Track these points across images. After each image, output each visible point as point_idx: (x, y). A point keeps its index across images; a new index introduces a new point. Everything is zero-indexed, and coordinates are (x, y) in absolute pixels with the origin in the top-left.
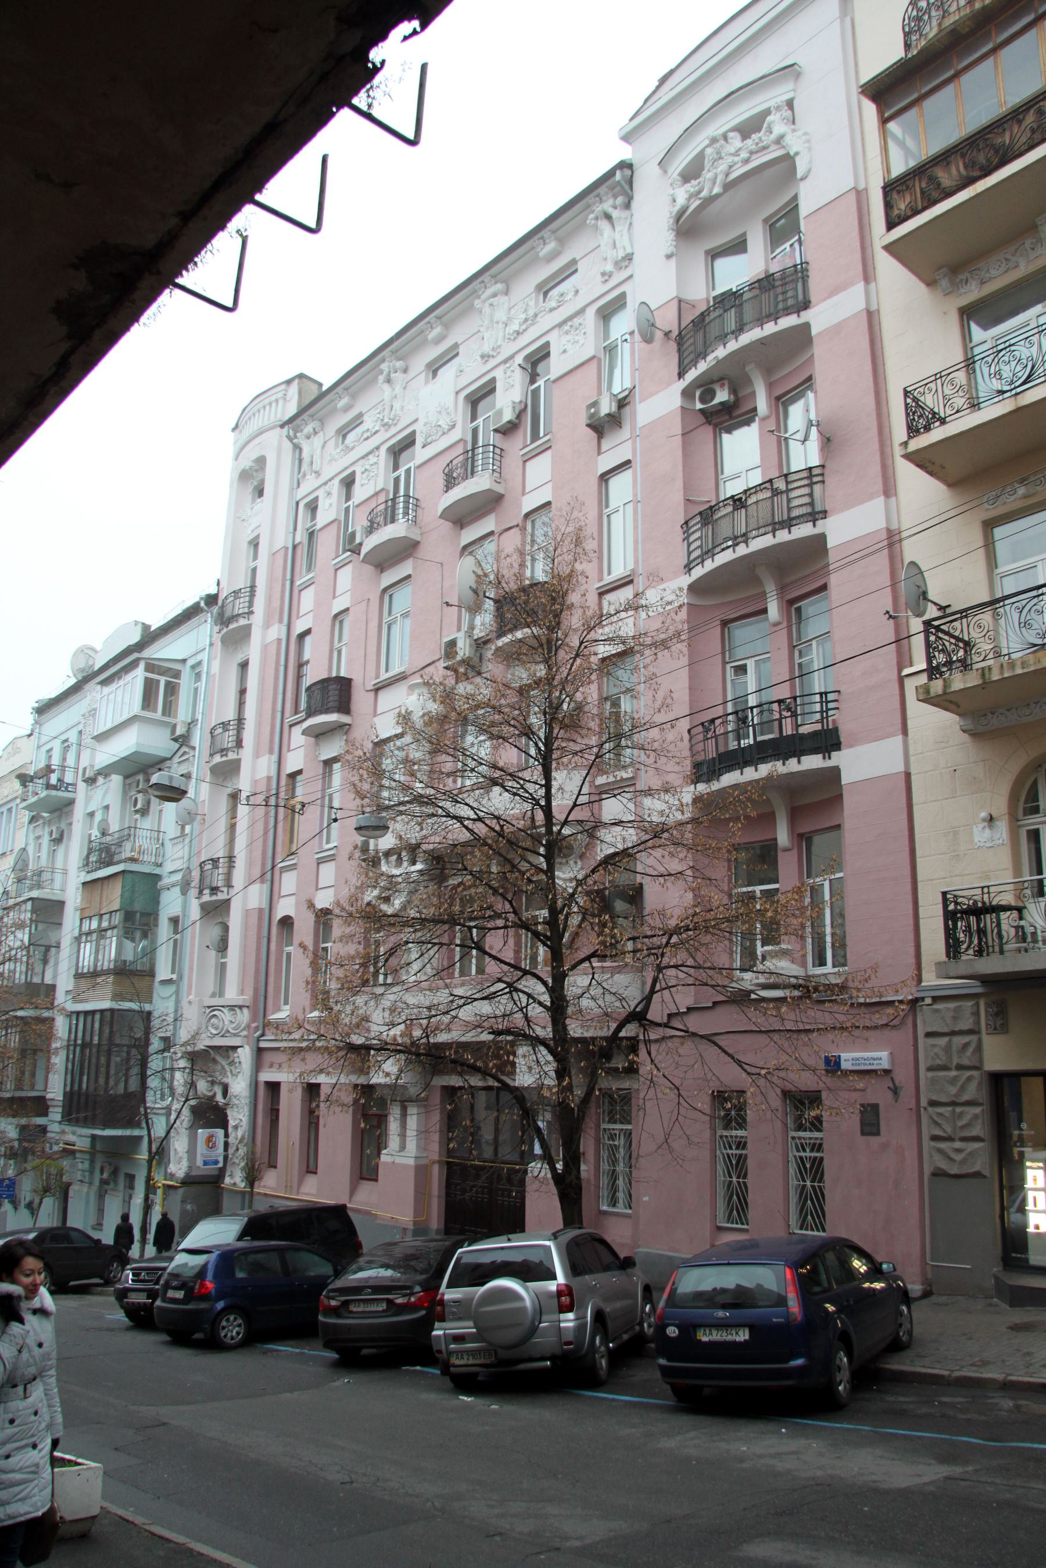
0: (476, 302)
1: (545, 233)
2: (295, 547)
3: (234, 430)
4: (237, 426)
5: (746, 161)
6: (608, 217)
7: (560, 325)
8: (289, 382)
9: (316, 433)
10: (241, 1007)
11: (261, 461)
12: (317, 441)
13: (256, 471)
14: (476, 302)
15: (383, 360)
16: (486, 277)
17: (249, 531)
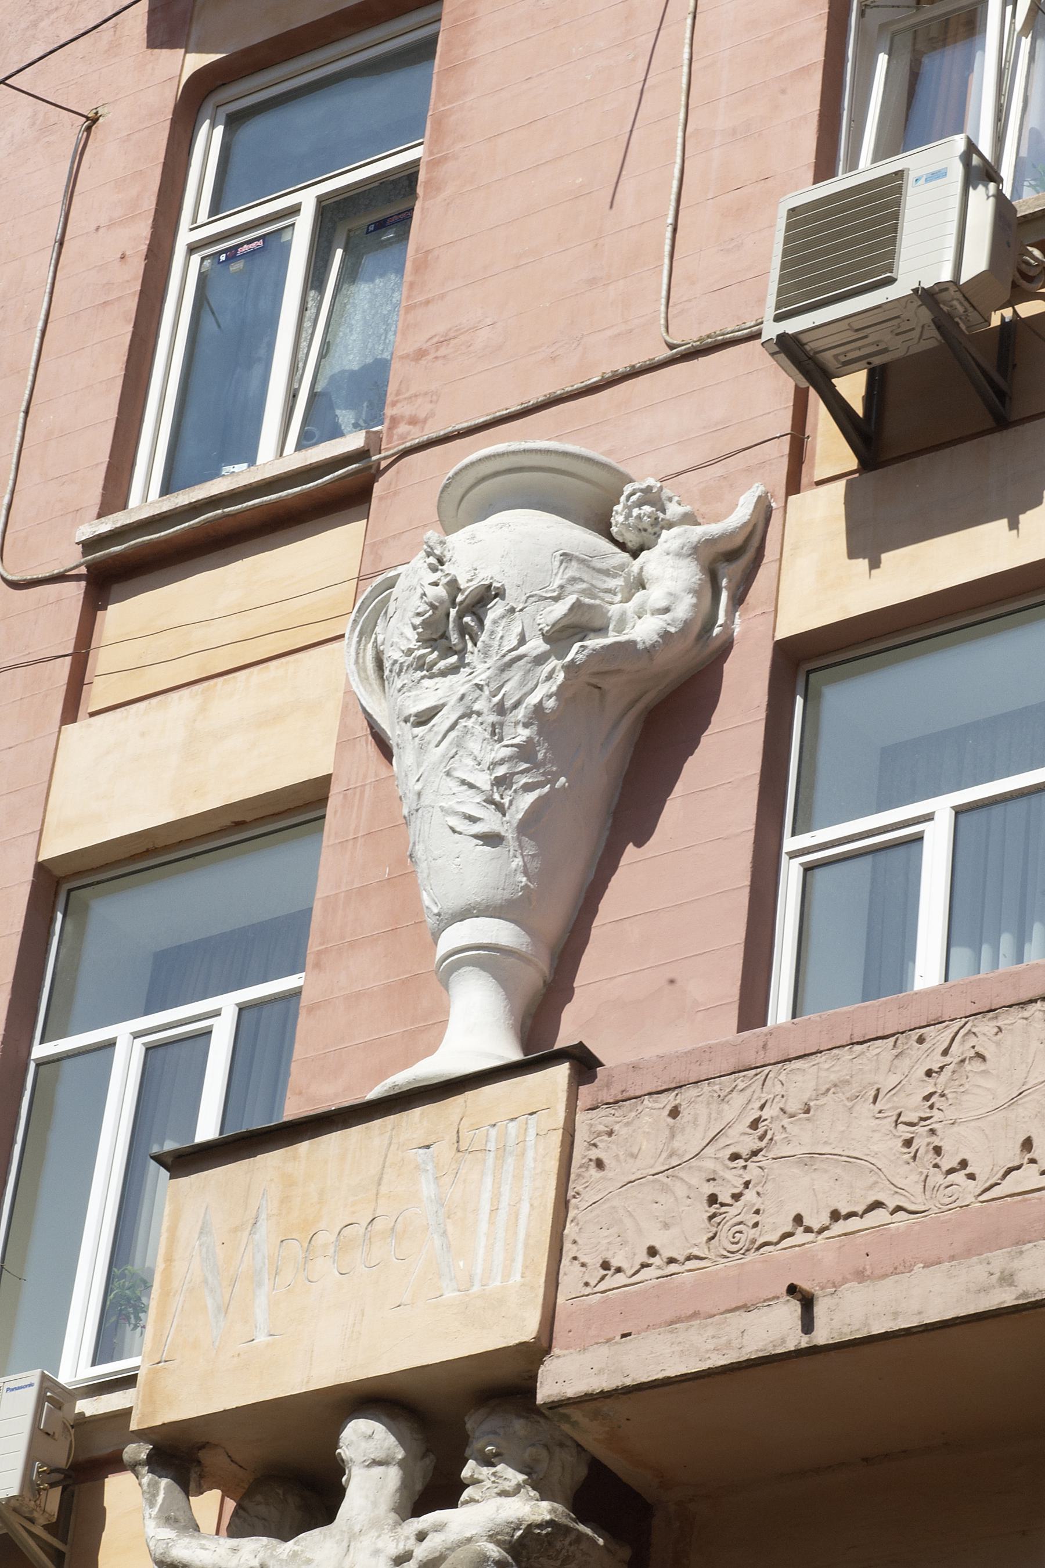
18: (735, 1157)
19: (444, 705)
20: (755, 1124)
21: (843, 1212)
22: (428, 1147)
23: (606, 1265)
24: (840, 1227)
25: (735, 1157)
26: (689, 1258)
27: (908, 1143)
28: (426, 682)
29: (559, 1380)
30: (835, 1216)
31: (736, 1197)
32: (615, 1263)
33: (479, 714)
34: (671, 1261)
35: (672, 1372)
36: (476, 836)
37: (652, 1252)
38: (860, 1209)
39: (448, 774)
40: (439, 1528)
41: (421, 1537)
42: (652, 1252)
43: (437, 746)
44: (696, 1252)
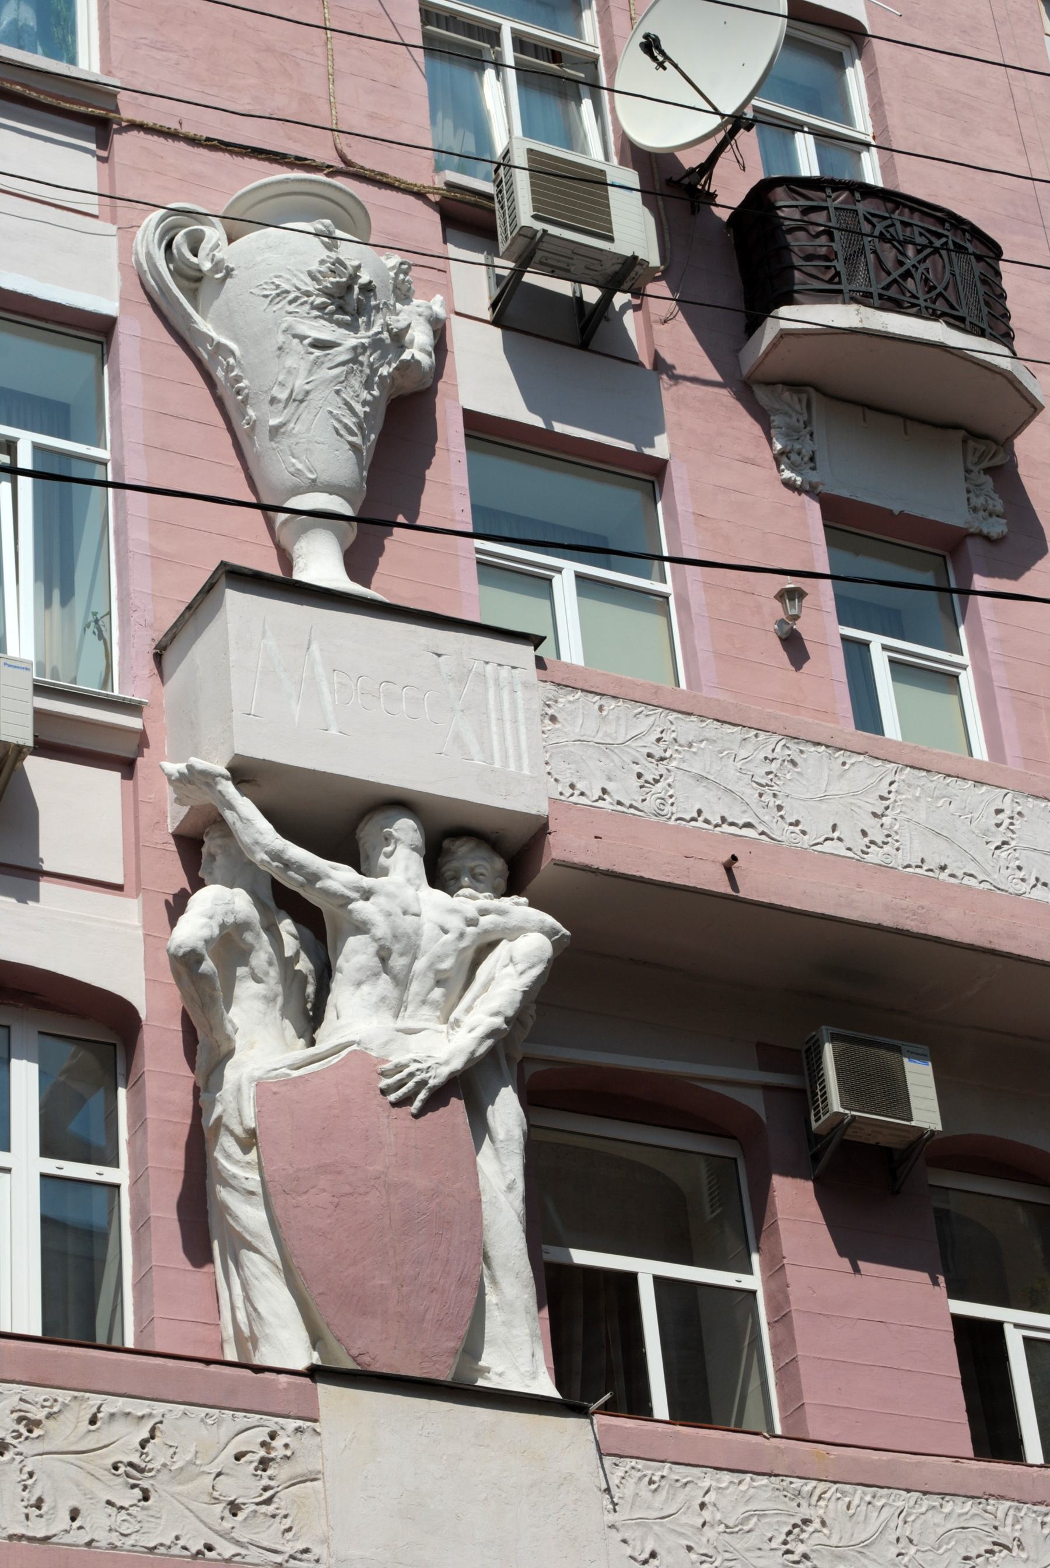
18: (649, 755)
19: (338, 345)
20: (659, 740)
21: (730, 820)
22: (439, 655)
23: (572, 786)
24: (725, 828)
25: (649, 755)
26: (631, 806)
27: (761, 795)
28: (323, 322)
30: (723, 819)
31: (657, 781)
32: (580, 786)
33: (361, 364)
34: (619, 803)
35: (647, 875)
36: (350, 443)
37: (604, 791)
38: (741, 822)
39: (338, 392)
40: (501, 912)
41: (484, 912)
42: (604, 791)
43: (330, 368)
44: (635, 804)
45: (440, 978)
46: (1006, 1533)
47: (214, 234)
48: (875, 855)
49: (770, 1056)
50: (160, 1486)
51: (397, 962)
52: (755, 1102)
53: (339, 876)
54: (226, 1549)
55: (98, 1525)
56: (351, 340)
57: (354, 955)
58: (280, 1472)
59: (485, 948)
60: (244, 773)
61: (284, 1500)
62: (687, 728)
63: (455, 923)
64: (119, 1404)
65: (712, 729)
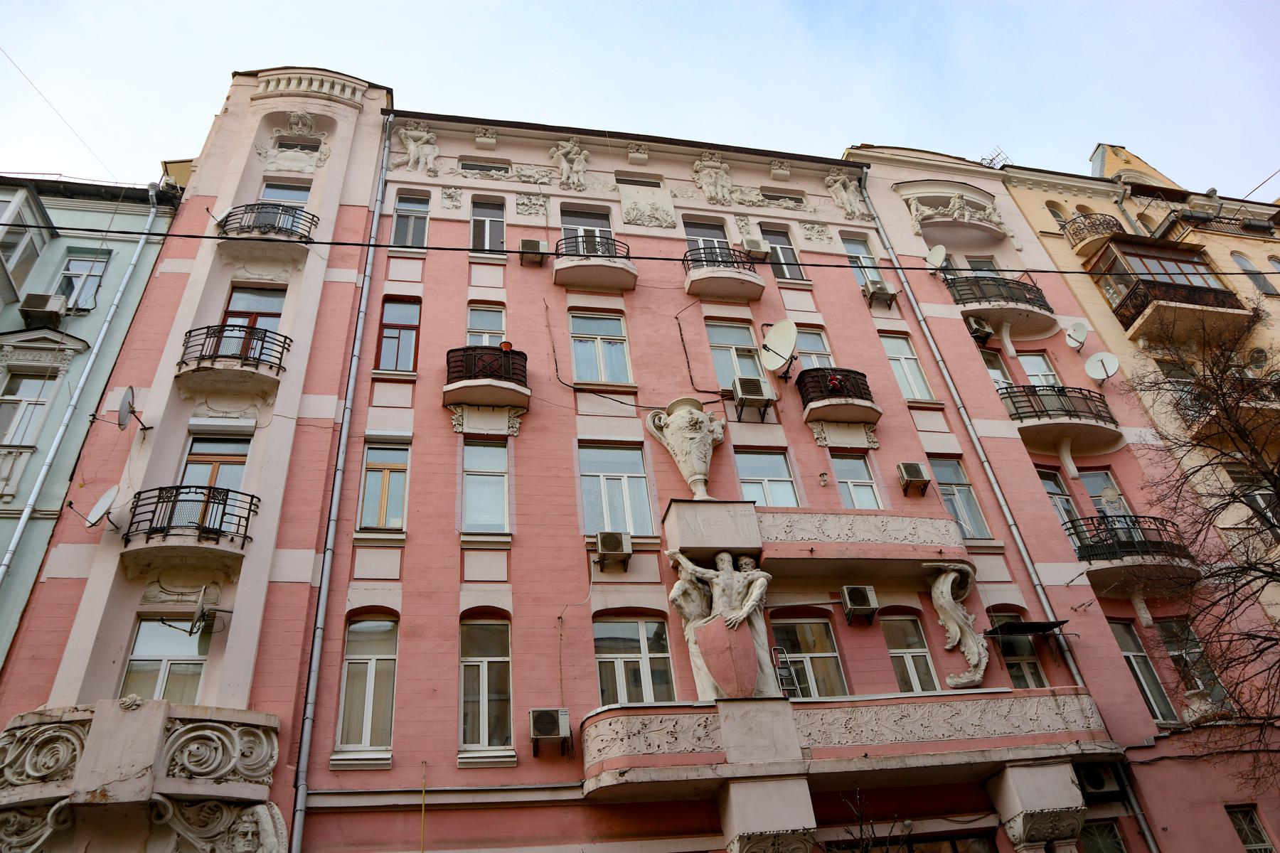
0: (697, 162)
1: (787, 162)
2: (381, 216)
3: (235, 74)
4: (253, 74)
5: (980, 220)
6: (845, 186)
7: (801, 221)
8: (372, 86)
9: (428, 142)
10: (268, 730)
11: (326, 124)
12: (429, 152)
13: (304, 125)
14: (697, 162)
15: (568, 140)
16: (718, 153)
17: (272, 167)
29: (765, 555)
45: (739, 592)
46: (905, 713)
47: (664, 416)
48: (851, 540)
49: (833, 595)
50: (679, 736)
51: (727, 592)
52: (830, 608)
53: (709, 573)
54: (698, 750)
55: (665, 748)
56: (698, 436)
57: (717, 592)
58: (710, 728)
59: (751, 583)
60: (683, 551)
61: (711, 735)
62: (796, 517)
63: (742, 580)
64: (666, 717)
65: (803, 516)
